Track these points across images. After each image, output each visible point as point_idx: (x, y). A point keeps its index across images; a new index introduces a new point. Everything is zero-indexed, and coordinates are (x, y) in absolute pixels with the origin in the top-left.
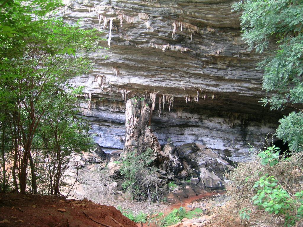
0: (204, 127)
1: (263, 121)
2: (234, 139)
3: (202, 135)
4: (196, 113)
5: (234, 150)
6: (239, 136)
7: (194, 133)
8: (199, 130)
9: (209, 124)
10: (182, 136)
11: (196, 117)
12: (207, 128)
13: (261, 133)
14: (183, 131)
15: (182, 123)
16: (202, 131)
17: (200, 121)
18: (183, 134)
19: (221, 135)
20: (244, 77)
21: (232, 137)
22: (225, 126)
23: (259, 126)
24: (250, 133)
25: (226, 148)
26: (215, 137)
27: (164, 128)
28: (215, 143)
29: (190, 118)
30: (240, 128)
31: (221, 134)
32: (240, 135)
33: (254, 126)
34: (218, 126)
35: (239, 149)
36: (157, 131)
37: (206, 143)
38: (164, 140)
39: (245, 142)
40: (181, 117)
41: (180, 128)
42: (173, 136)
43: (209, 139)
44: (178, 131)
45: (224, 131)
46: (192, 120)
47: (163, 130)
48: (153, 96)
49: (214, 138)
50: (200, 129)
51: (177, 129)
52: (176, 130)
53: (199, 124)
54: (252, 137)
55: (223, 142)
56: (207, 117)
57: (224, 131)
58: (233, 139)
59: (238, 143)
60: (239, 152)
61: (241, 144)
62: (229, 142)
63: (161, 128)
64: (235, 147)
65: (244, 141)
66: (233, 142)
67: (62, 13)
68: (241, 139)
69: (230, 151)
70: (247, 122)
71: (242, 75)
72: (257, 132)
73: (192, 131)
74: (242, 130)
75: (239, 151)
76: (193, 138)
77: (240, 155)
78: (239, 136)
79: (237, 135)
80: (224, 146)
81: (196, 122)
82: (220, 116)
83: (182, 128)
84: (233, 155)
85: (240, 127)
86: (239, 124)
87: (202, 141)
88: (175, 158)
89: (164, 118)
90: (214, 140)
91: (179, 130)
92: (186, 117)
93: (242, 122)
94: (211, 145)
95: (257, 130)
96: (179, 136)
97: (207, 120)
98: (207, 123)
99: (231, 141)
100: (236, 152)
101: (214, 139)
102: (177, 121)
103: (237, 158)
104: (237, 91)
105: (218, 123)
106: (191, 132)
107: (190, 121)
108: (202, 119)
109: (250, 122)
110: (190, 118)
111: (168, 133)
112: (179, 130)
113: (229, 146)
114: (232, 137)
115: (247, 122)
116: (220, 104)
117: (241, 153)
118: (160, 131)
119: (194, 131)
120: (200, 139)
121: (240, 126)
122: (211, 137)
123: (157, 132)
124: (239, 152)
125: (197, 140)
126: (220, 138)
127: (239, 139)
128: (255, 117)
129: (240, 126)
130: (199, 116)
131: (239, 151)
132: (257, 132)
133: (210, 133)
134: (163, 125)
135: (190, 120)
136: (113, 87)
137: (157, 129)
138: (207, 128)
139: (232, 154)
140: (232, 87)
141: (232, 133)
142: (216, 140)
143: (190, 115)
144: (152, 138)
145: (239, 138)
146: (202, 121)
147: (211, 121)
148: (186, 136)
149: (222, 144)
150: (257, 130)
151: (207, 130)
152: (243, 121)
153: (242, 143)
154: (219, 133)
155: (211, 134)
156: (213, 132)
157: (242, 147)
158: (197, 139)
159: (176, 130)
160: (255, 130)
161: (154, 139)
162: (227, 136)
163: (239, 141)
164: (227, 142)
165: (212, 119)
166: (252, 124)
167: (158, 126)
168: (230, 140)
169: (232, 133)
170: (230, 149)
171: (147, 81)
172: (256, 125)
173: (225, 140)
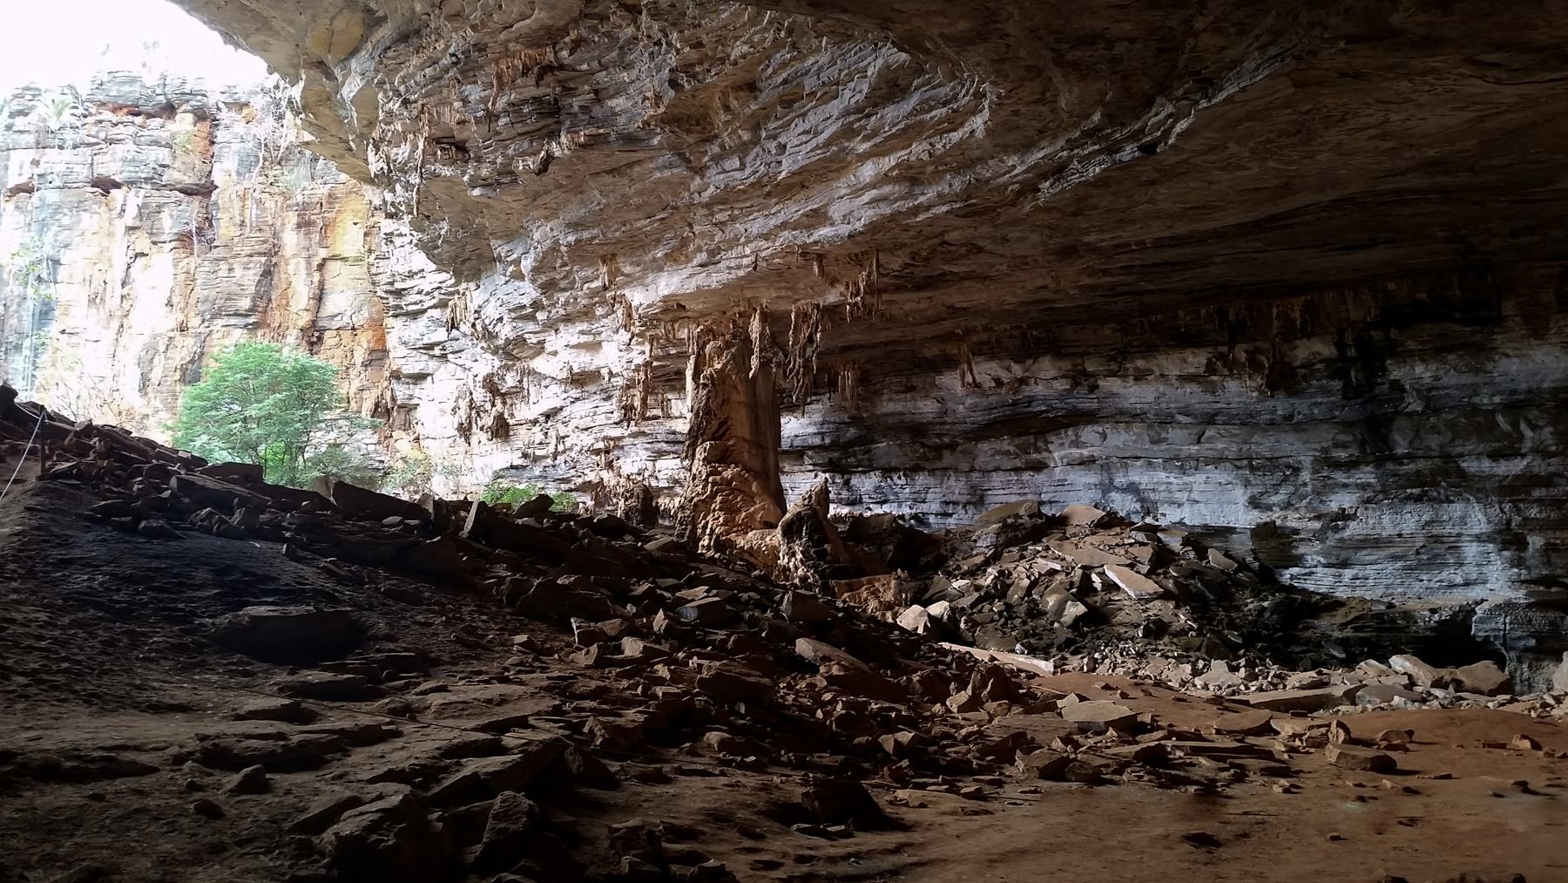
0: (1122, 412)
1: (1508, 307)
2: (1316, 460)
3: (1126, 461)
4: (1044, 354)
5: (1317, 525)
6: (1342, 437)
7: (1085, 452)
8: (1104, 436)
9: (1135, 394)
10: (1041, 478)
11: (1052, 373)
12: (1131, 417)
13: (1514, 392)
14: (1038, 450)
15: (995, 414)
16: (1121, 439)
17: (1083, 390)
18: (1039, 467)
19: (1220, 446)
20: (813, 143)
21: (1298, 444)
22: (1238, 391)
23: (1478, 351)
24: (1417, 406)
25: (1265, 517)
26: (1190, 457)
27: (952, 447)
28: (1195, 496)
29: (1023, 381)
30: (1337, 384)
31: (1220, 442)
32: (1346, 425)
33: (1437, 351)
34: (1192, 395)
35: (1353, 517)
36: (927, 465)
37: (1152, 495)
38: (969, 503)
39: (1390, 466)
40: (977, 385)
41: (1017, 441)
42: (997, 479)
43: (1162, 475)
44: (1008, 453)
45: (1247, 421)
46: (1039, 389)
47: (948, 458)
48: (755, 326)
49: (1184, 464)
50: (1107, 428)
51: (1006, 444)
52: (998, 452)
53: (1088, 404)
54: (1434, 430)
55: (1247, 484)
56: (1112, 359)
57: (1247, 421)
58: (1307, 461)
59: (1340, 477)
60: (1347, 534)
61: (1363, 487)
62: (1286, 479)
63: (938, 449)
64: (1324, 509)
65: (1379, 463)
66: (1305, 476)
68: (1354, 451)
69: (1296, 531)
70: (1377, 335)
71: (804, 138)
72: (1475, 390)
73: (1077, 444)
74: (1349, 393)
75: (1353, 529)
76: (1093, 478)
77: (1363, 555)
78: (1342, 437)
79: (1326, 436)
80: (1254, 503)
81: (1062, 396)
82: (1185, 340)
83: (1031, 439)
84: (1312, 553)
85: (1331, 377)
86: (1327, 361)
87: (1132, 489)
88: (794, 554)
89: (920, 404)
90: (1186, 479)
91: (1012, 449)
92: (999, 382)
93: (1341, 346)
94: (1180, 505)
95: (1467, 379)
96: (1026, 476)
97: (1113, 374)
98: (1121, 391)
99: (1296, 470)
100: (1332, 539)
101: (1183, 470)
102: (973, 408)
103: (1348, 573)
104: (886, 210)
105: (1185, 379)
106: (1075, 452)
107: (1031, 400)
108: (1087, 375)
109: (1394, 333)
110: (1023, 381)
111: (972, 470)
112: (1012, 449)
113: (1288, 505)
114: (1300, 450)
115: (1377, 335)
116: (1086, 281)
117: (1374, 543)
118: (938, 465)
119: (1082, 445)
120: (1120, 480)
121: (1336, 369)
122: (1166, 460)
123: (932, 472)
124: (1347, 534)
125: (1107, 487)
126: (1217, 461)
127: (1342, 454)
128: (1423, 296)
129: (1336, 369)
130: (1066, 365)
131: (1353, 529)
132: (1475, 390)
133: (1153, 442)
134: (939, 436)
135: (1027, 391)
136: (656, 327)
137: (924, 458)
138: (1131, 417)
139: (1302, 550)
140: (858, 202)
141: (1289, 423)
142: (1200, 478)
143: (1017, 370)
144: (706, 480)
145: (1344, 446)
146: (1093, 388)
147: (1140, 377)
148: (1058, 473)
149: (1240, 495)
150: (1467, 379)
151: (1137, 427)
152: (1349, 338)
153: (1366, 475)
154: (1210, 432)
155: (1164, 446)
156: (1174, 434)
157: (1369, 501)
158: (1111, 481)
159: (998, 452)
160: (1452, 379)
161: (714, 483)
162: (1263, 445)
163: (1350, 465)
164: (1269, 480)
165: (1140, 363)
166: (1411, 345)
167: (923, 445)
168: (1288, 466)
169: (1298, 428)
170: (1294, 524)
171: (691, 276)
172: (1451, 349)
173: (1253, 469)
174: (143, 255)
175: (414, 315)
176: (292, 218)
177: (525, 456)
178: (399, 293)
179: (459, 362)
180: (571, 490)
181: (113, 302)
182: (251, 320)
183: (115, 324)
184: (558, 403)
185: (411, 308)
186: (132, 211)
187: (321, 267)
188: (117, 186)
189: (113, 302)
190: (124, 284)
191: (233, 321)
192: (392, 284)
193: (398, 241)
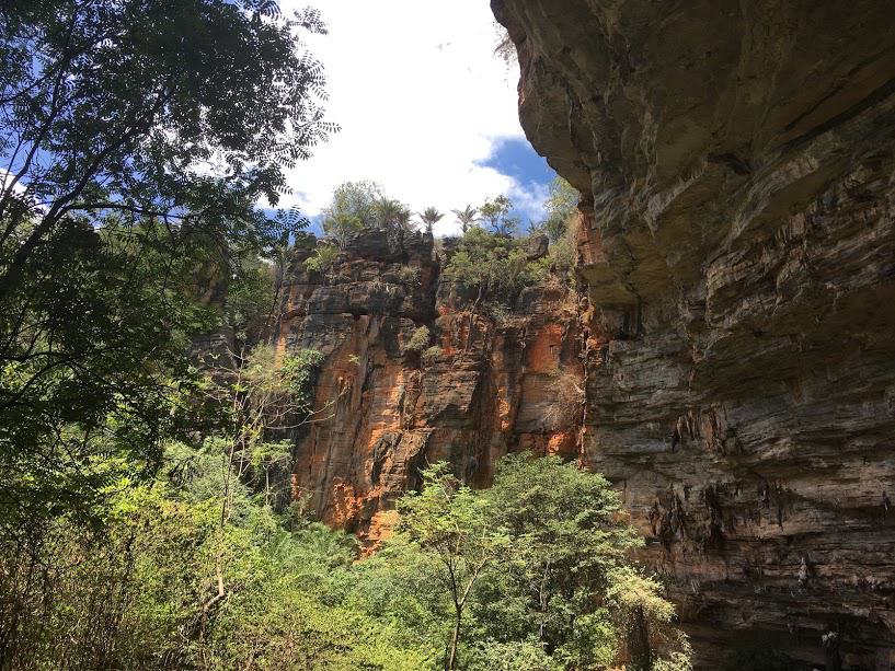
67: (802, 262)
174: (379, 366)
175: (620, 428)
176: (501, 342)
177: (747, 572)
178: (613, 407)
179: (670, 472)
180: (798, 614)
181: (355, 403)
182: (467, 422)
183: (355, 422)
184: (815, 527)
185: (622, 419)
186: (374, 333)
187: (521, 381)
188: (365, 312)
189: (355, 403)
190: (363, 390)
191: (453, 423)
192: (609, 398)
193: (627, 361)
